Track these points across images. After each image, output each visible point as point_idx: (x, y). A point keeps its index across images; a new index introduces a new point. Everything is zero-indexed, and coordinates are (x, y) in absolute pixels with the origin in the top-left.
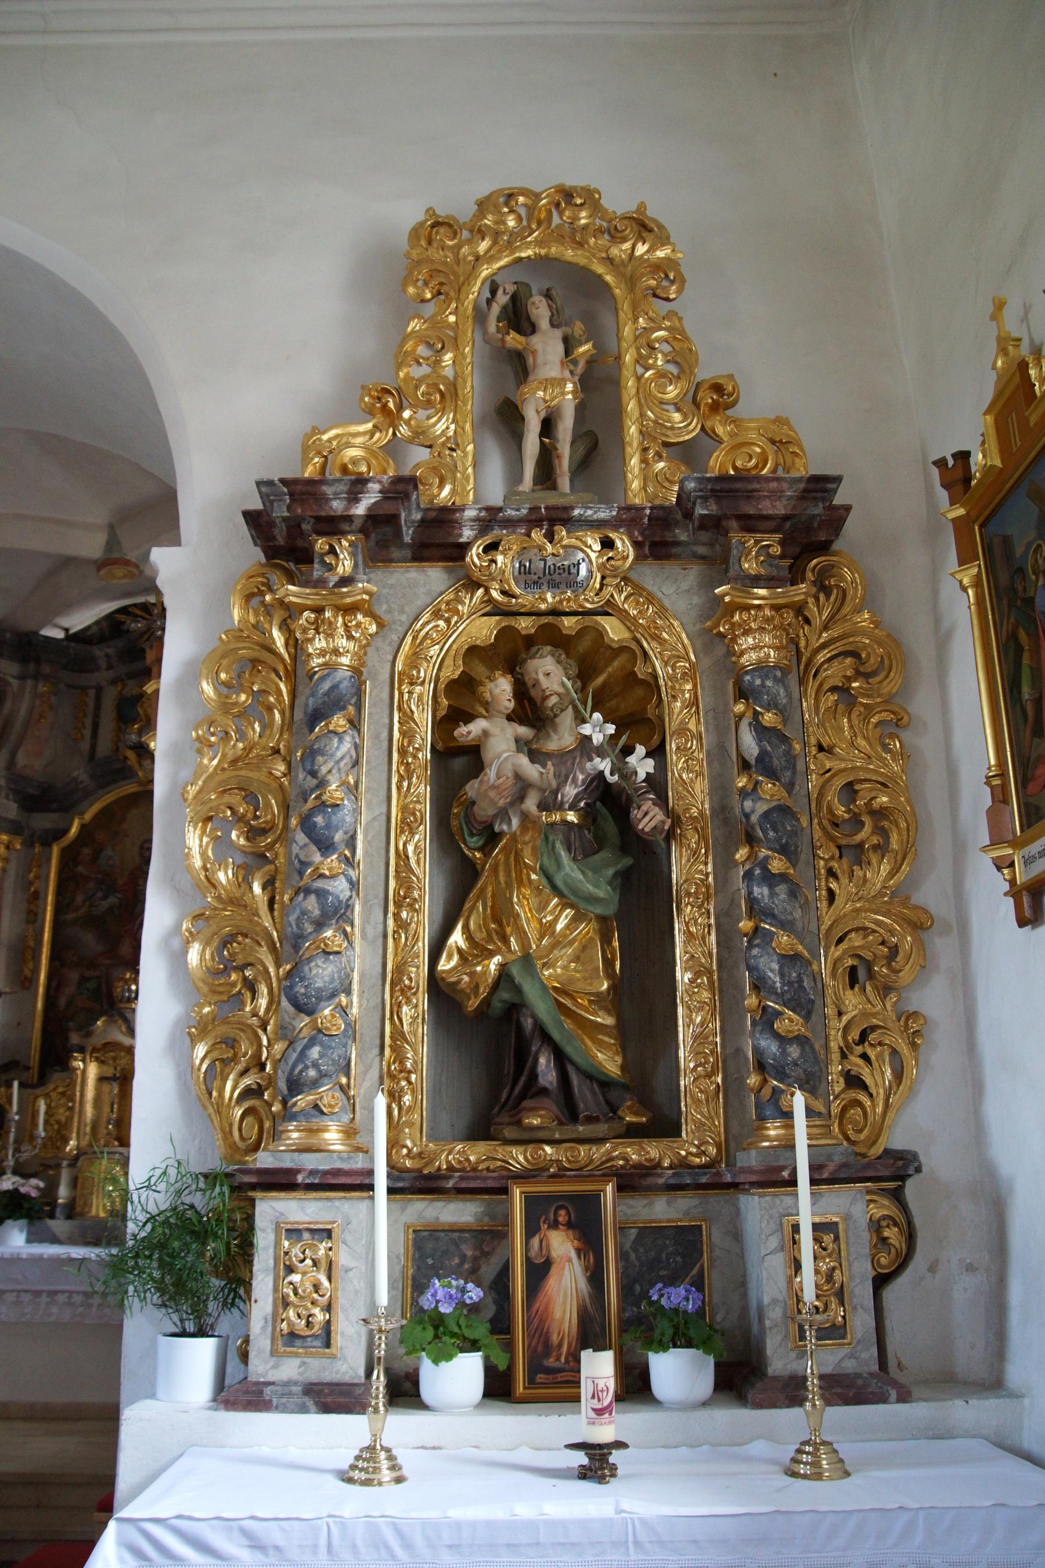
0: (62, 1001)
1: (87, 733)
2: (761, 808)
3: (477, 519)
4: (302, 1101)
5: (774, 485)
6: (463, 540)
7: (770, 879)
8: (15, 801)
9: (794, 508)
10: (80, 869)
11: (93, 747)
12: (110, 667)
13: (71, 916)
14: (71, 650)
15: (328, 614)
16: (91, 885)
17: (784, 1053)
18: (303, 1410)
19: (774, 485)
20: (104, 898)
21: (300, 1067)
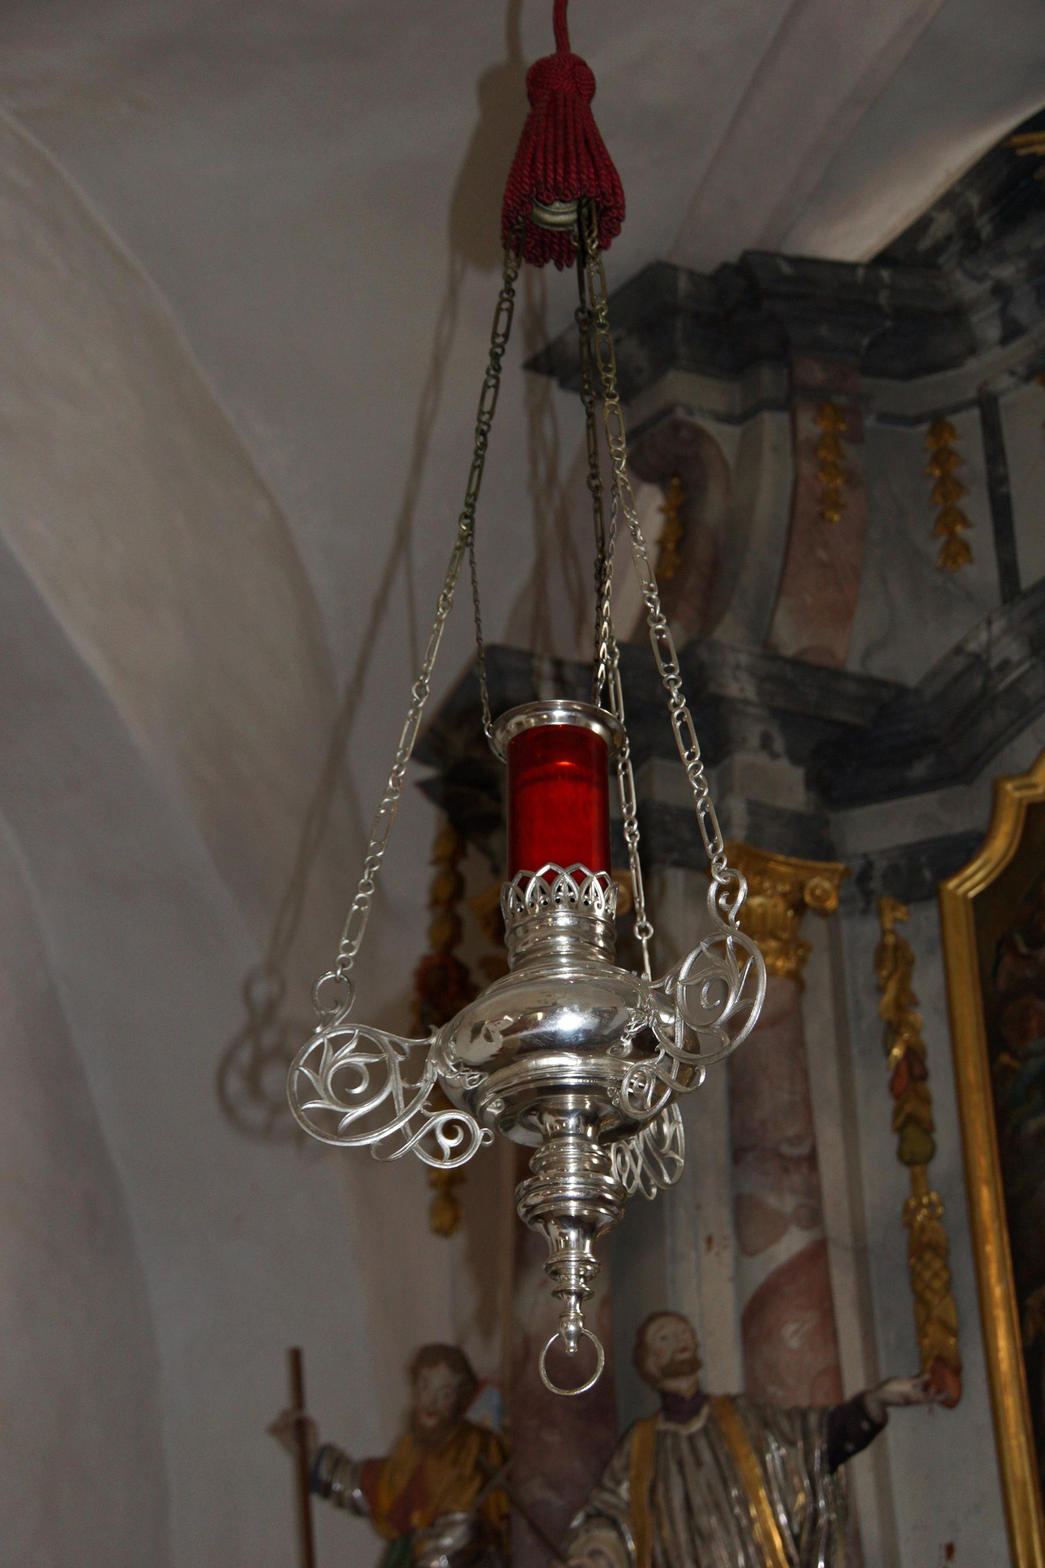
8: (795, 759)
11: (1008, 571)
14: (883, 298)
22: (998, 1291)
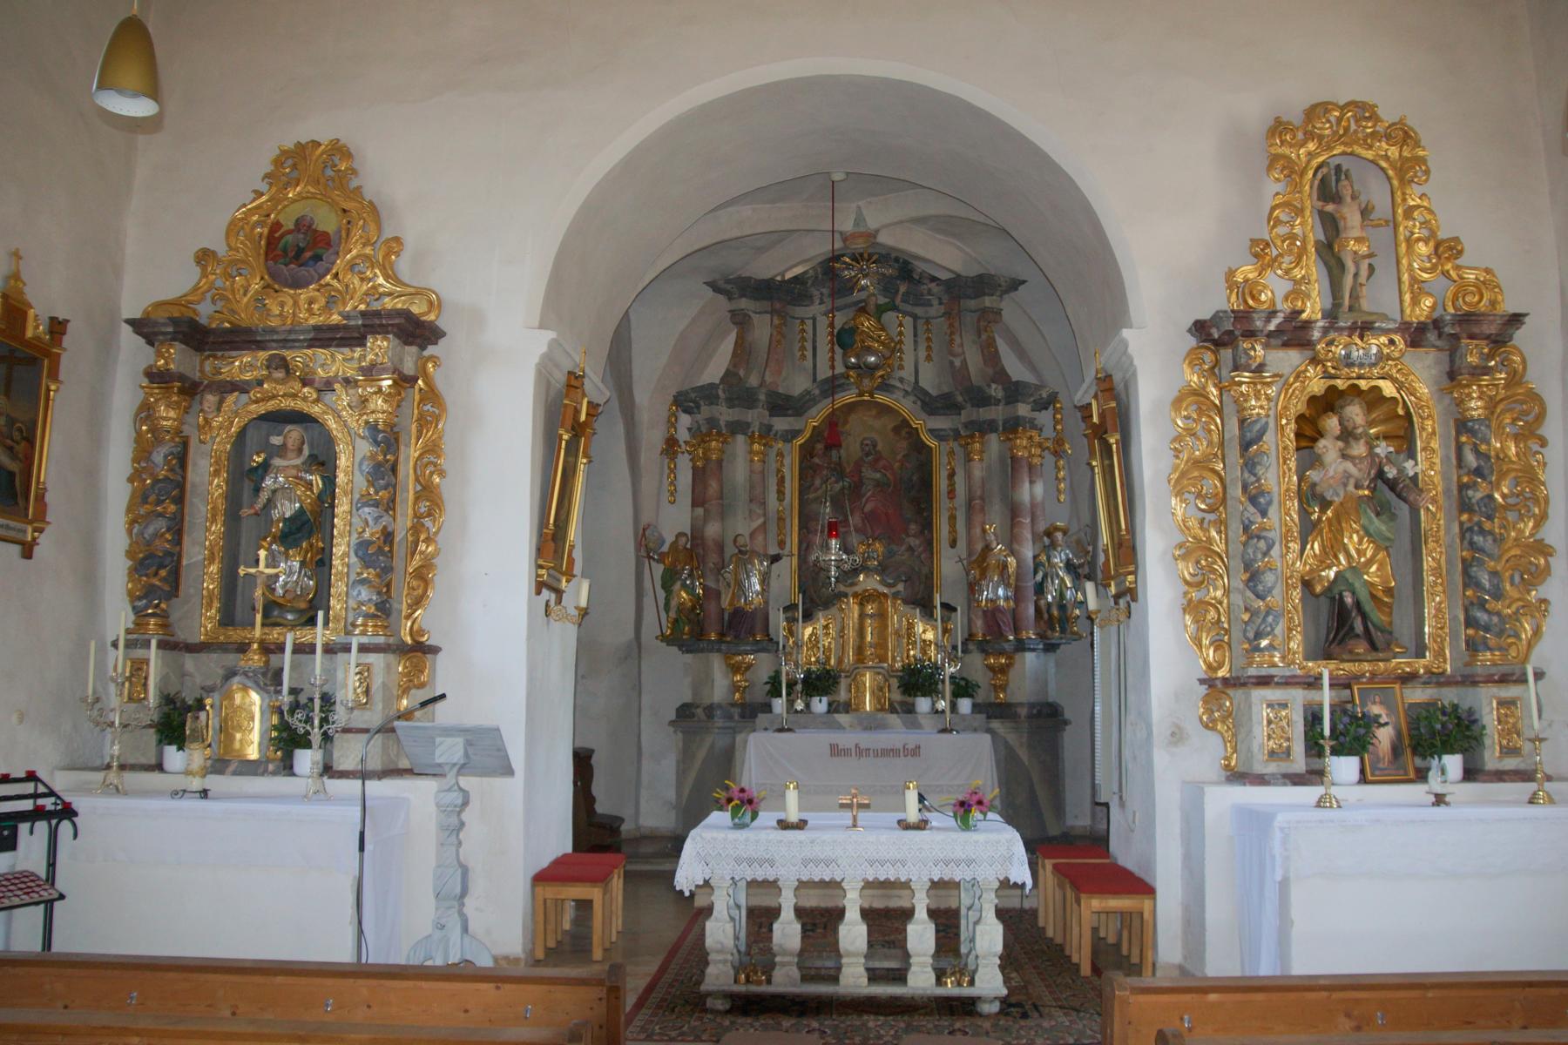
1: (809, 354)
2: (1479, 495)
3: (1324, 327)
4: (1264, 643)
5: (1491, 318)
6: (1314, 338)
7: (1482, 532)
9: (1501, 329)
10: (816, 460)
13: (812, 496)
15: (1259, 387)
17: (1491, 620)
18: (1285, 784)
19: (1491, 318)
20: (837, 482)
21: (1263, 626)
22: (796, 528)
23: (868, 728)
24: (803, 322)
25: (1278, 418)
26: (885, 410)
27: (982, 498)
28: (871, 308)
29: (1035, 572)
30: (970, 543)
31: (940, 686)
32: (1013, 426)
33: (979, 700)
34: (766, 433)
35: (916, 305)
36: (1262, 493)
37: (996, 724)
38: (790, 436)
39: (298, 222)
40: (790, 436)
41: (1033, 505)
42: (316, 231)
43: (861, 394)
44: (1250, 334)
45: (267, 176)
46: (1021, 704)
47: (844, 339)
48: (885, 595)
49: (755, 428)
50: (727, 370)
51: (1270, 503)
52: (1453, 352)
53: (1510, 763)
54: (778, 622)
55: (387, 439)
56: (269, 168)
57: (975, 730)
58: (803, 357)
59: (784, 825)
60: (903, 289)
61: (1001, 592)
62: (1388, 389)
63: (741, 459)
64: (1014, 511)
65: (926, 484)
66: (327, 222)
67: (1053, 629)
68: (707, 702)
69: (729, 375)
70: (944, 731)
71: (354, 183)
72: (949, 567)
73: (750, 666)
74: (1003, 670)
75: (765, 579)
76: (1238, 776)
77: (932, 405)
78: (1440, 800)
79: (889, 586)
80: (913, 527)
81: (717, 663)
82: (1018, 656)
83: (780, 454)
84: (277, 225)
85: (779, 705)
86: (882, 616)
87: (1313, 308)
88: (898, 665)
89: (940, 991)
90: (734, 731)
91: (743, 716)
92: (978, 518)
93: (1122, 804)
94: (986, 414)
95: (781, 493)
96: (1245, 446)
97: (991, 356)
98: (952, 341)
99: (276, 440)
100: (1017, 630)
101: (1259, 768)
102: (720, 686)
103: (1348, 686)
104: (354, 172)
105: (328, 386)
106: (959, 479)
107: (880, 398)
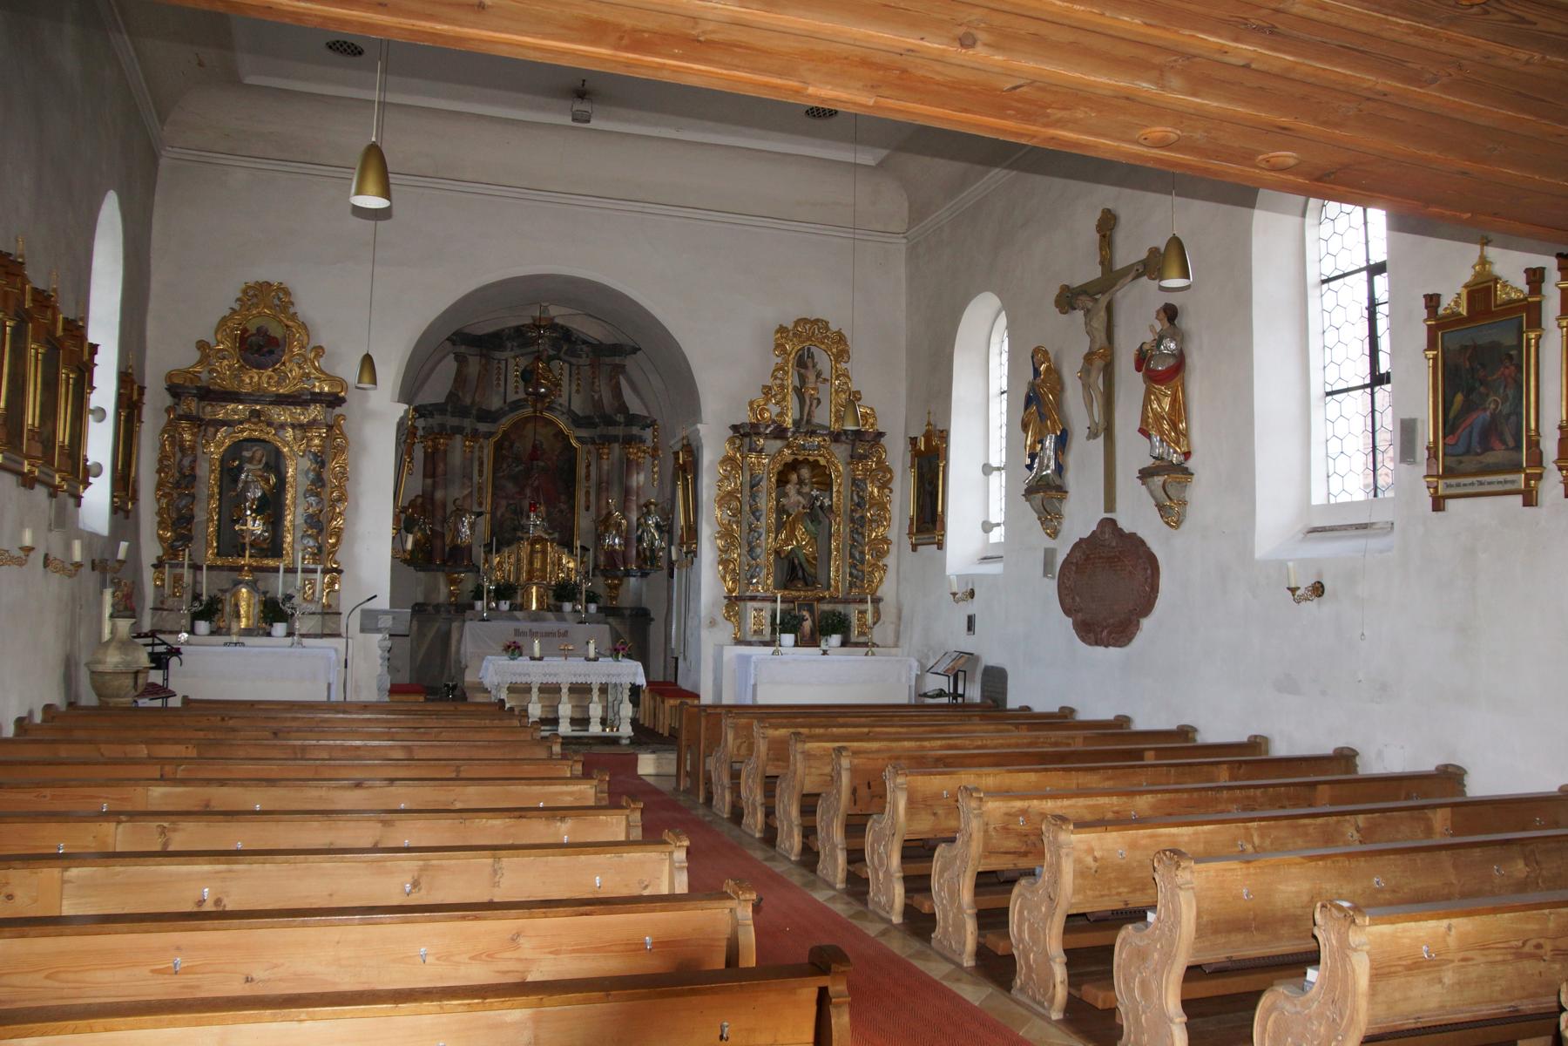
0: (499, 514)
1: (502, 383)
2: (858, 516)
4: (754, 581)
7: (858, 533)
10: (504, 452)
12: (512, 350)
16: (510, 460)
23: (536, 620)
24: (499, 363)
25: (769, 473)
26: (550, 423)
27: (608, 483)
28: (544, 357)
29: (638, 530)
30: (598, 510)
31: (578, 596)
32: (629, 440)
33: (601, 605)
34: (475, 435)
35: (573, 356)
36: (757, 510)
37: (610, 620)
38: (488, 435)
39: (259, 330)
40: (488, 435)
41: (638, 488)
42: (269, 336)
43: (535, 411)
44: (758, 434)
45: (238, 300)
46: (626, 608)
47: (528, 376)
48: (547, 540)
49: (468, 430)
50: (450, 392)
51: (761, 515)
52: (853, 446)
53: (862, 639)
54: (479, 553)
55: (320, 461)
56: (240, 295)
57: (598, 623)
58: (498, 385)
59: (532, 658)
60: (565, 348)
61: (617, 541)
62: (822, 462)
63: (457, 450)
64: (626, 492)
65: (572, 470)
66: (276, 331)
67: (646, 564)
68: (436, 602)
69: (452, 396)
70: (581, 622)
71: (292, 310)
72: (584, 522)
73: (462, 580)
74: (616, 587)
75: (472, 526)
76: (739, 642)
77: (577, 421)
78: (825, 653)
79: (549, 534)
80: (563, 497)
81: (441, 579)
82: (625, 579)
83: (481, 447)
84: (245, 331)
85: (479, 605)
86: (544, 552)
87: (789, 422)
88: (553, 583)
89: (603, 734)
90: (451, 621)
91: (457, 611)
92: (604, 495)
93: (685, 659)
94: (612, 431)
95: (481, 472)
96: (752, 487)
97: (617, 392)
98: (593, 383)
99: (247, 454)
100: (625, 564)
101: (749, 638)
102: (443, 592)
103: (793, 602)
104: (292, 304)
105: (282, 426)
106: (593, 469)
107: (547, 414)
